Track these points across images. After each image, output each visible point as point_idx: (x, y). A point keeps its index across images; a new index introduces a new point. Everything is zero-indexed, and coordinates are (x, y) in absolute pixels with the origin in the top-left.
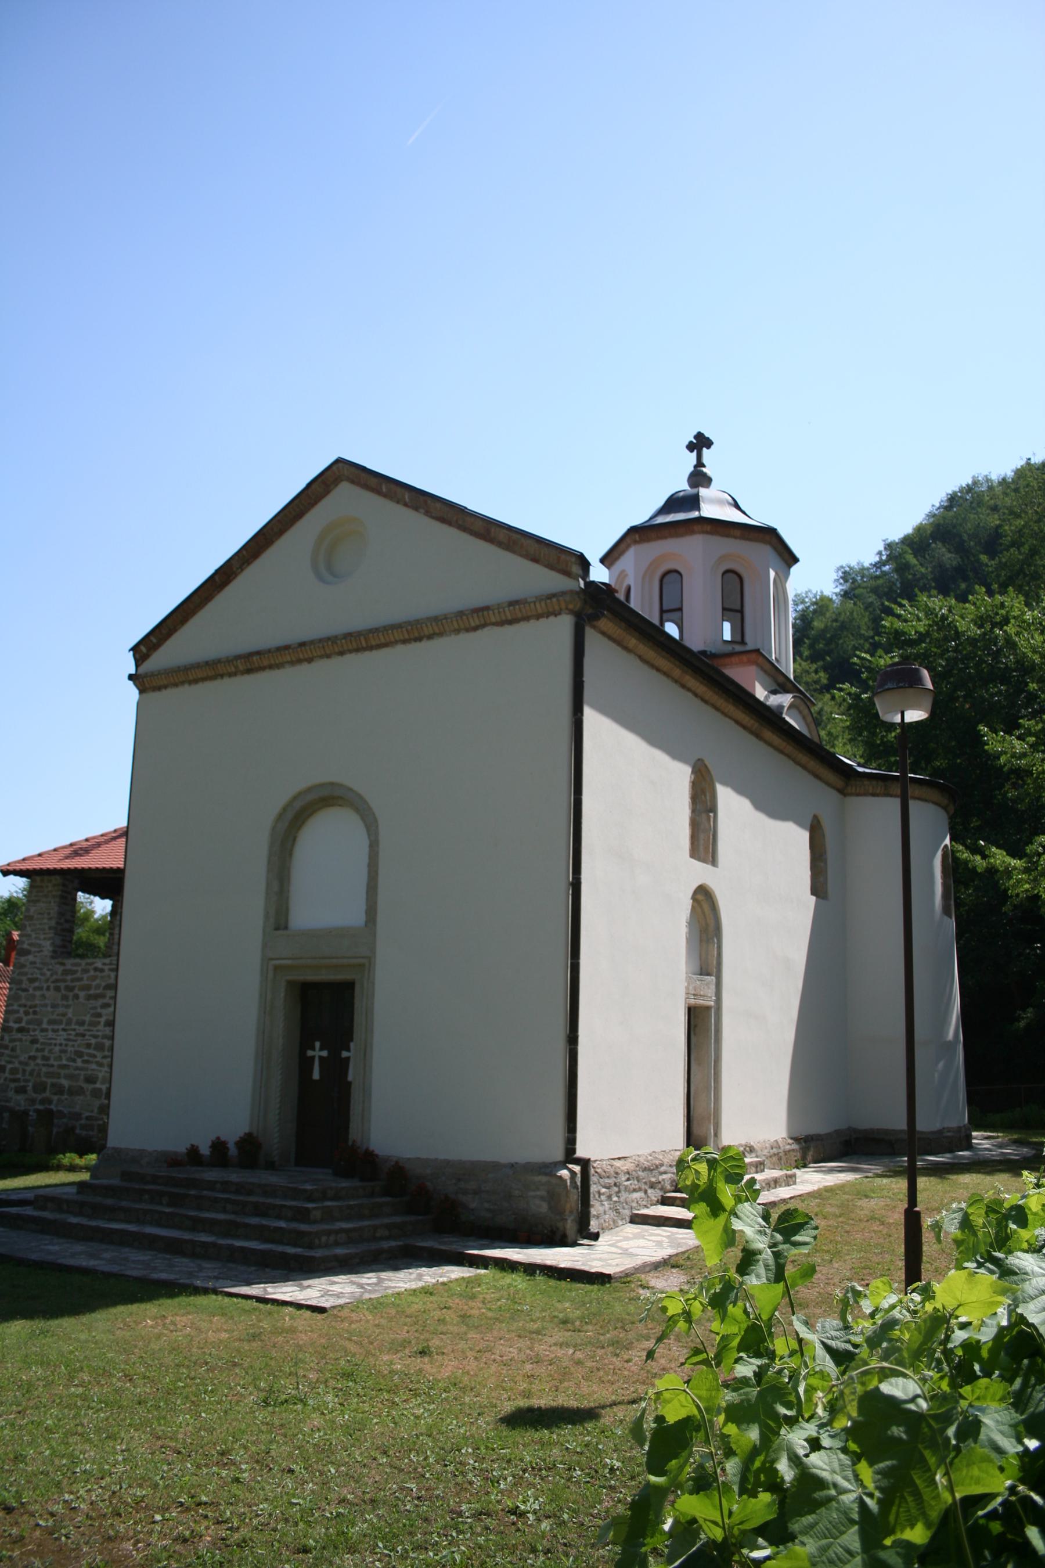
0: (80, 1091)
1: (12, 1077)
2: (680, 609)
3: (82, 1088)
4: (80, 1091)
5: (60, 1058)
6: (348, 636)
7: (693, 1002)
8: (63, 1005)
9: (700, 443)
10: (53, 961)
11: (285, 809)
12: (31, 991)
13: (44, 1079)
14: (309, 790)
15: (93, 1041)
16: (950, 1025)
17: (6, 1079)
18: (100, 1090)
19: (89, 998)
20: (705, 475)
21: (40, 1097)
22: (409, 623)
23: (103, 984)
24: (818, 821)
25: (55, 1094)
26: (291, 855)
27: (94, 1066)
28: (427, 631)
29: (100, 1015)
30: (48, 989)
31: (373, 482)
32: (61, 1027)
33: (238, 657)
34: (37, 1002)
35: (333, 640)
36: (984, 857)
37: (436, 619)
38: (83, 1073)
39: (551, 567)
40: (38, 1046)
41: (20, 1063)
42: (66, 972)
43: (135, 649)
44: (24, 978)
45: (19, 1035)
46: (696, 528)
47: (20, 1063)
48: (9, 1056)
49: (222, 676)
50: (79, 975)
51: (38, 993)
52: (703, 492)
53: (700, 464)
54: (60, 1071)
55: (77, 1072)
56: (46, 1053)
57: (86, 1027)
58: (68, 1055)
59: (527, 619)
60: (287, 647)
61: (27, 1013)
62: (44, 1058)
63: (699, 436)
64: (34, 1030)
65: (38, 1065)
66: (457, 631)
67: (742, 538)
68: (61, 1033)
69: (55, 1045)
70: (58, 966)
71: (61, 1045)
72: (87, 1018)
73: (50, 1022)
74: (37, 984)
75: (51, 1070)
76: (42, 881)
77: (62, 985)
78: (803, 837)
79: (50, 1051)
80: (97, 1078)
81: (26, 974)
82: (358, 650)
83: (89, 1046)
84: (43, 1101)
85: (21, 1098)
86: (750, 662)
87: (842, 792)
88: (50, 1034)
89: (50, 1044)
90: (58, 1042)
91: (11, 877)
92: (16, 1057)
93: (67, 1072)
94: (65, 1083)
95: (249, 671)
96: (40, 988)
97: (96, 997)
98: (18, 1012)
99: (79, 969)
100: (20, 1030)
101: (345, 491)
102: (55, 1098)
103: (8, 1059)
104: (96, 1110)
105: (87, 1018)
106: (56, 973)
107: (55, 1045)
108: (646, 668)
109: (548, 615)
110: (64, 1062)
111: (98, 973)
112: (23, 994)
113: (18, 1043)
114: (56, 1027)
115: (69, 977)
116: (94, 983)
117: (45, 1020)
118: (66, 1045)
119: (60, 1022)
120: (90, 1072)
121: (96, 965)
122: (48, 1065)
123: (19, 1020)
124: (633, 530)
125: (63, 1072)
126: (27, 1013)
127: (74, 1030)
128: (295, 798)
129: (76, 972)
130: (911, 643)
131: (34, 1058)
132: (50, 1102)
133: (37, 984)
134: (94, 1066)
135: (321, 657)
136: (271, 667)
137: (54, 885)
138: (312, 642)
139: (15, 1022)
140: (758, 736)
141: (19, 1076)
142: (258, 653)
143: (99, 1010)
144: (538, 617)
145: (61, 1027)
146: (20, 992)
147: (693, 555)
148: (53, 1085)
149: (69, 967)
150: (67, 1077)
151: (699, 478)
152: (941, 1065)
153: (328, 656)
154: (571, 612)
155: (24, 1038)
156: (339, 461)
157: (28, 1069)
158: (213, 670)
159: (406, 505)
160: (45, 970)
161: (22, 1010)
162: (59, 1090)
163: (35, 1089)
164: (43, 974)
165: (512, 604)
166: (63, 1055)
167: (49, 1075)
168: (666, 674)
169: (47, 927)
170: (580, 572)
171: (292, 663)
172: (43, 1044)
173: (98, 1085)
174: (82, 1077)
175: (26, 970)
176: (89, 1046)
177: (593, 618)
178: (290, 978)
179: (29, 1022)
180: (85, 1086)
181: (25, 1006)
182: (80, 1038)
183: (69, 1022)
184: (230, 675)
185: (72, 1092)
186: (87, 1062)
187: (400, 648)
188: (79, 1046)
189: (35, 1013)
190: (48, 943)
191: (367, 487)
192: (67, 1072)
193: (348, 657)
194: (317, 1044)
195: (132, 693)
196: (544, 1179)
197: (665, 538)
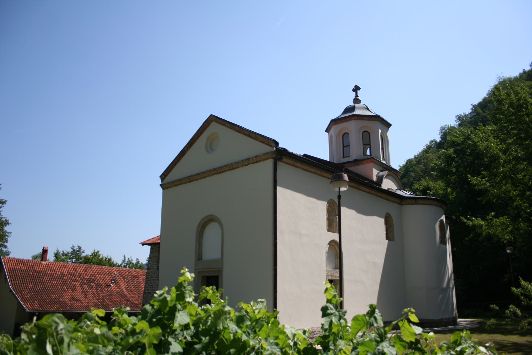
2: (349, 146)
6: (214, 169)
7: (330, 278)
9: (356, 89)
11: (200, 223)
14: (206, 217)
16: (444, 281)
20: (358, 99)
22: (230, 164)
24: (390, 215)
26: (202, 237)
31: (220, 121)
33: (186, 178)
36: (472, 221)
37: (236, 163)
39: (267, 144)
43: (161, 176)
46: (352, 118)
49: (183, 183)
52: (356, 105)
53: (357, 96)
59: (260, 161)
60: (198, 174)
63: (356, 86)
66: (242, 166)
67: (369, 120)
78: (382, 220)
82: (217, 173)
86: (371, 162)
87: (400, 204)
91: (145, 246)
95: (190, 182)
100: (149, 293)
101: (214, 124)
108: (305, 172)
123: (148, 290)
124: (332, 121)
128: (203, 220)
130: (458, 145)
136: (195, 180)
138: (205, 172)
140: (358, 189)
142: (191, 176)
144: (263, 160)
147: (352, 127)
151: (357, 100)
152: (441, 296)
153: (210, 176)
154: (272, 158)
156: (211, 116)
158: (190, 179)
165: (256, 157)
168: (314, 173)
170: (275, 145)
177: (280, 159)
179: (151, 290)
184: (185, 183)
187: (228, 172)
191: (218, 123)
193: (215, 176)
195: (161, 190)
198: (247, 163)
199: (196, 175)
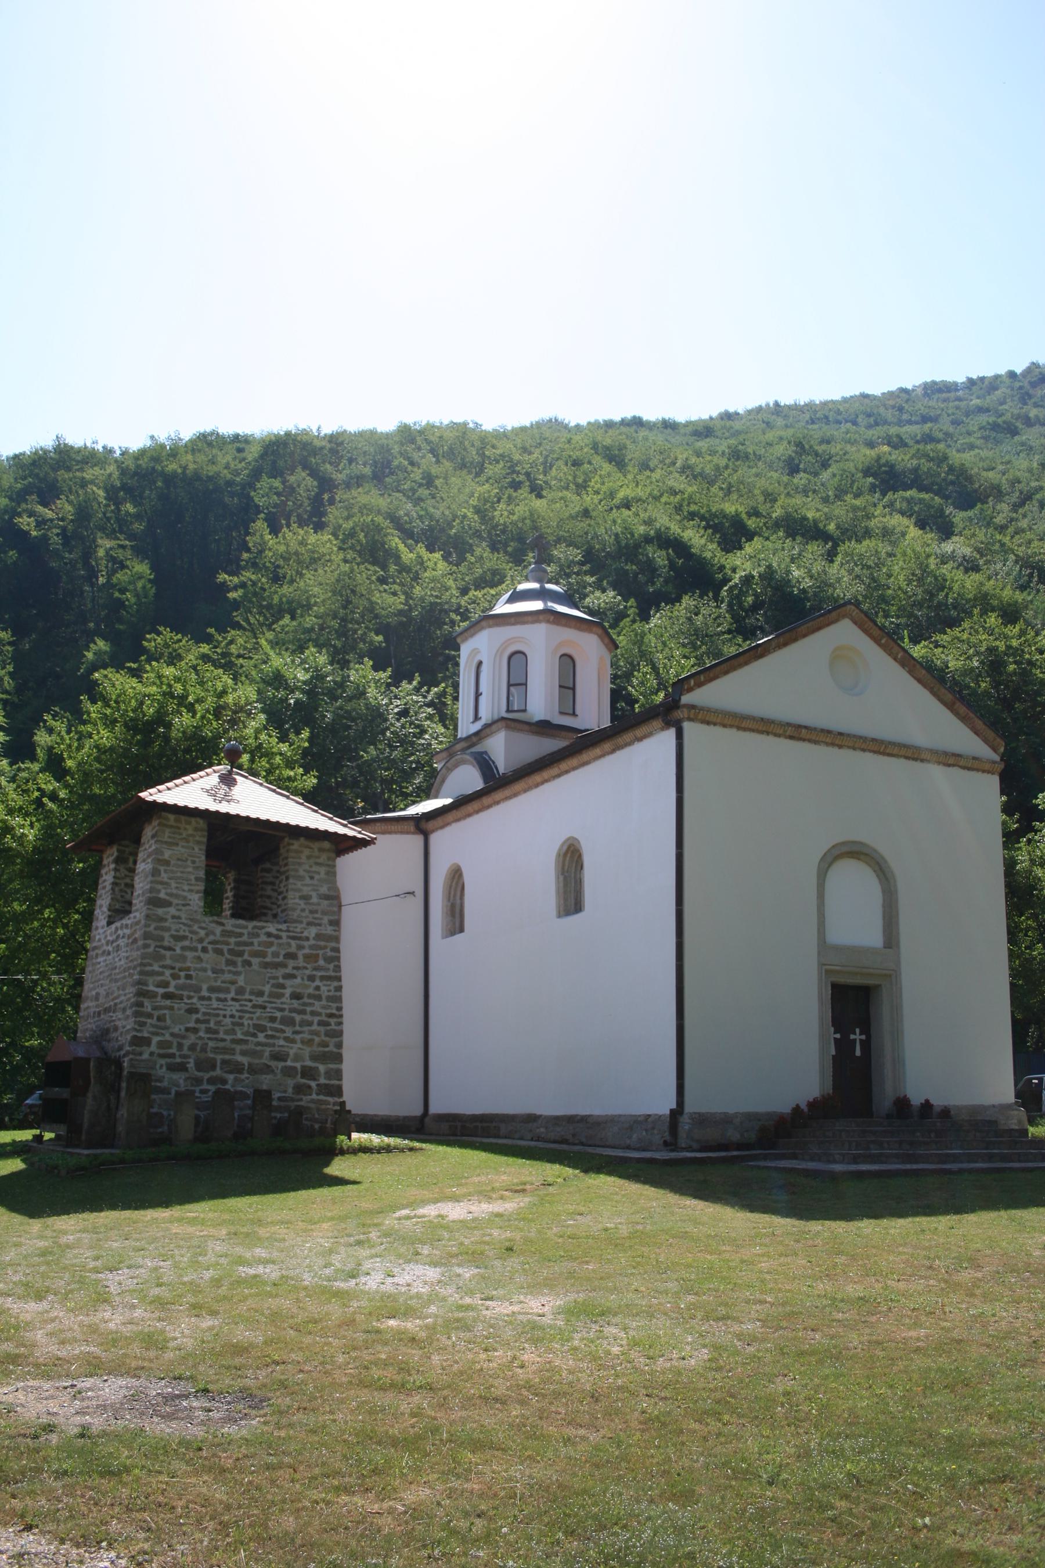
0: (268, 1069)
1: (162, 1051)
3: (269, 1067)
4: (268, 1069)
5: (234, 1032)
6: (874, 740)
8: (230, 972)
10: (207, 919)
12: (178, 951)
13: (212, 1056)
15: (278, 1014)
17: (152, 1054)
18: (295, 1068)
19: (266, 965)
21: (207, 1076)
23: (283, 952)
25: (231, 1072)
27: (282, 1042)
28: (923, 756)
29: (283, 987)
30: (205, 950)
32: (229, 996)
33: (789, 724)
34: (189, 964)
35: (864, 739)
38: (268, 1049)
40: (199, 1016)
41: (172, 1035)
42: (226, 933)
44: (166, 935)
45: (168, 1002)
47: (172, 1035)
48: (153, 1026)
49: (768, 733)
50: (245, 938)
51: (189, 954)
54: (234, 1046)
55: (259, 1048)
56: (212, 1025)
57: (265, 998)
58: (246, 1029)
59: (978, 770)
60: (829, 732)
61: (175, 977)
62: (209, 1030)
64: (190, 997)
65: (201, 1038)
68: (230, 1003)
69: (225, 1016)
70: (213, 925)
71: (232, 1016)
72: (267, 989)
73: (211, 989)
74: (186, 943)
76: (176, 820)
77: (225, 948)
79: (218, 1023)
80: (288, 1055)
81: (168, 929)
83: (273, 1019)
84: (211, 1081)
85: (179, 1077)
88: (215, 1004)
89: (218, 1015)
90: (228, 1013)
92: (166, 1028)
93: (244, 1047)
94: (245, 1060)
95: (791, 737)
96: (195, 949)
97: (276, 966)
98: (162, 974)
99: (245, 931)
100: (167, 996)
102: (231, 1077)
103: (151, 1029)
104: (290, 1090)
105: (267, 989)
106: (214, 934)
107: (225, 1016)
109: (989, 772)
110: (240, 1036)
111: (272, 939)
112: (168, 953)
113: (165, 1012)
114: (222, 996)
115: (232, 940)
116: (270, 950)
117: (205, 987)
118: (241, 1018)
119: (227, 991)
120: (277, 1049)
121: (267, 930)
122: (216, 1039)
125: (238, 1048)
126: (175, 977)
127: (251, 1001)
129: (241, 935)
131: (195, 1030)
132: (224, 1082)
133: (186, 943)
134: (282, 1042)
135: (849, 747)
136: (810, 741)
137: (196, 829)
139: (158, 986)
141: (173, 1051)
142: (806, 727)
143: (281, 981)
144: (984, 771)
145: (229, 996)
146: (163, 952)
148: (224, 1062)
149: (229, 928)
150: (243, 1053)
153: (854, 749)
155: (176, 1006)
157: (187, 1043)
159: (895, 659)
160: (195, 928)
161: (168, 972)
162: (238, 1068)
163: (199, 1066)
164: (196, 933)
165: (974, 758)
166: (237, 1028)
167: (215, 1050)
169: (192, 877)
171: (827, 744)
172: (205, 1014)
173: (289, 1063)
174: (267, 1054)
175: (167, 924)
176: (273, 1019)
178: (833, 979)
181: (173, 968)
182: (259, 1010)
183: (241, 991)
184: (776, 735)
185: (253, 1070)
186: (272, 1037)
187: (903, 760)
188: (258, 1019)
189: (188, 977)
190: (196, 896)
192: (244, 1047)
194: (858, 1031)
196: (1016, 1112)
197: (570, 627)
198: (951, 761)
199: (822, 730)
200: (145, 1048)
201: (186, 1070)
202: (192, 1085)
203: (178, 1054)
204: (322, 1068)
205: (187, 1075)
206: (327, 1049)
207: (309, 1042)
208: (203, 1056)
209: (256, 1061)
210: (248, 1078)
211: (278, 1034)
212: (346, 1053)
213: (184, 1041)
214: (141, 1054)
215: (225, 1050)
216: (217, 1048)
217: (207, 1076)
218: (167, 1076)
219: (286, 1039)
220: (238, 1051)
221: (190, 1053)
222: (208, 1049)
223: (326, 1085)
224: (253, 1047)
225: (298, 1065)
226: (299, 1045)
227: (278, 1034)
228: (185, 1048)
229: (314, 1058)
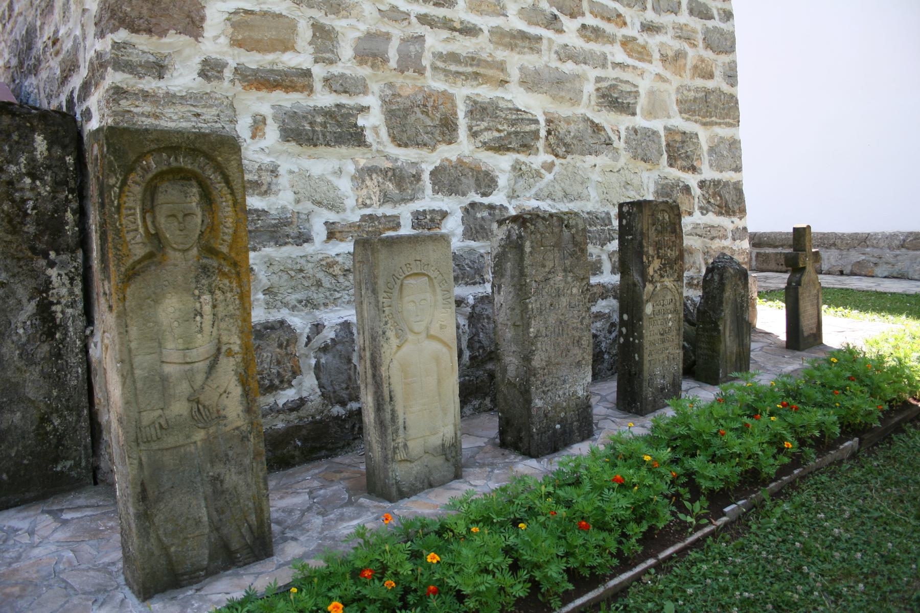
0: (596, 138)
1: (254, 60)
3: (597, 128)
13: (437, 84)
17: (210, 69)
21: (429, 160)
25: (500, 147)
38: (593, 73)
54: (501, 54)
55: (569, 67)
75: (464, 45)
84: (447, 180)
85: (332, 166)
102: (501, 164)
110: (517, 23)
120: (612, 73)
122: (447, 24)
125: (516, 62)
132: (486, 182)
134: (619, 55)
141: (299, 58)
148: (479, 110)
162: (516, 136)
163: (404, 123)
173: (640, 121)
174: (589, 88)
180: (608, 119)
192: (531, 60)
200: (173, 40)
201: (356, 137)
202: (386, 199)
203: (319, 71)
204: (704, 136)
205: (363, 159)
206: (710, 84)
207: (674, 60)
208: (408, 85)
209: (564, 111)
210: (549, 167)
211: (609, 28)
212: (743, 92)
213: (338, 23)
214: (159, 69)
215: (476, 69)
216: (453, 57)
217: (429, 160)
218: (285, 166)
219: (627, 43)
220: (515, 74)
221: (364, 71)
222: (426, 62)
223: (717, 183)
224: (555, 63)
225: (658, 125)
226: (656, 67)
227: (609, 28)
228: (346, 51)
229: (688, 108)
